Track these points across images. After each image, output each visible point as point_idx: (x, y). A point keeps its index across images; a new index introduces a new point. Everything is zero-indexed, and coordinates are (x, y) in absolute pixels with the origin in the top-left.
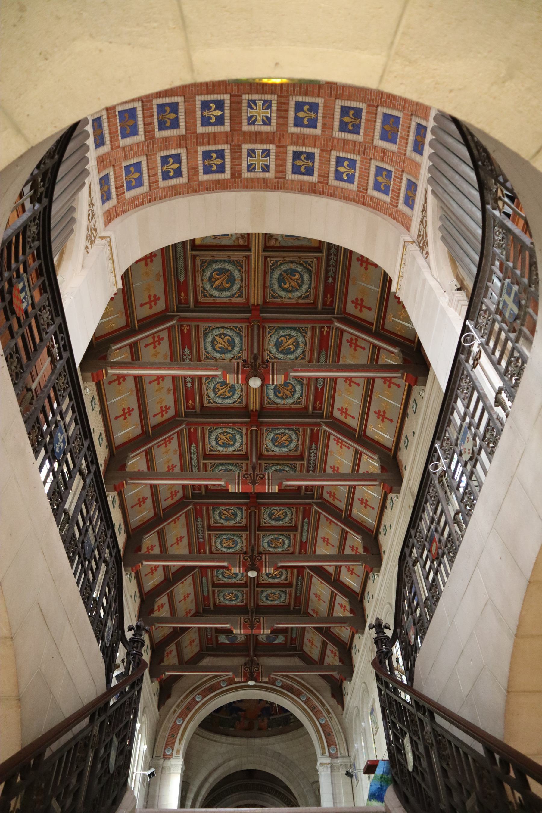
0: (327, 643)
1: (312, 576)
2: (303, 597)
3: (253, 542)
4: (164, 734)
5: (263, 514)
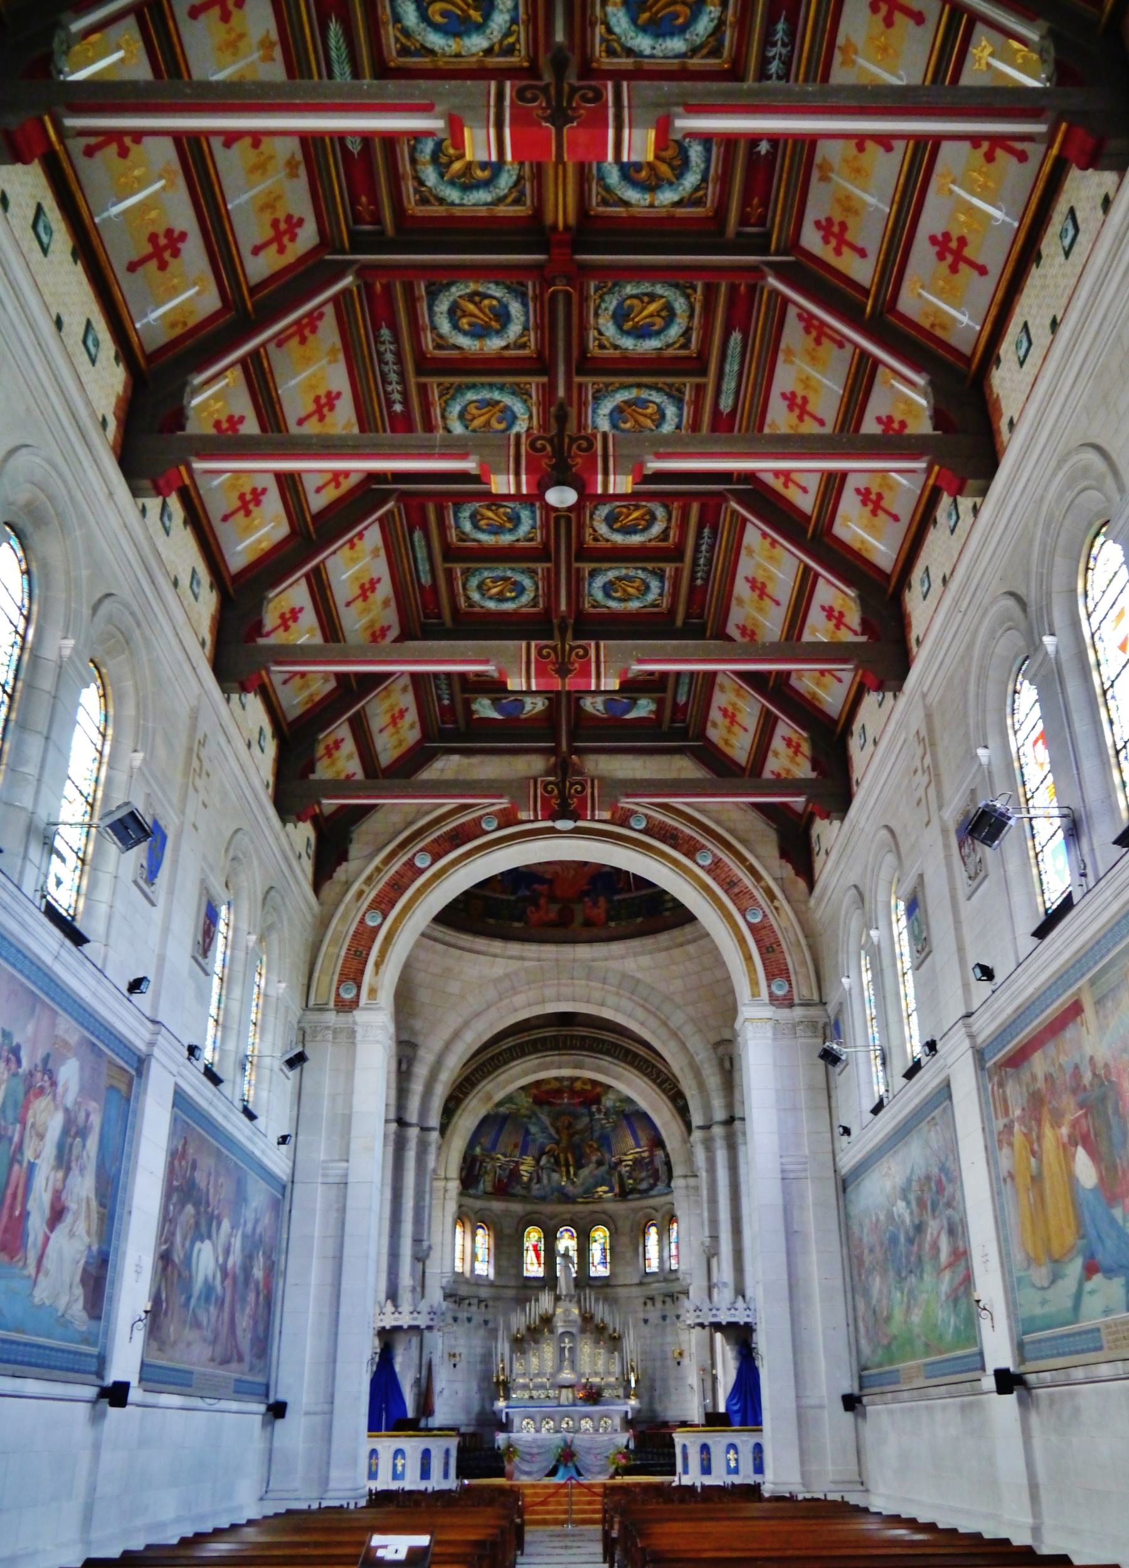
0: (777, 718)
1: (745, 521)
2: (715, 587)
3: (561, 393)
4: (334, 953)
5: (596, 315)
